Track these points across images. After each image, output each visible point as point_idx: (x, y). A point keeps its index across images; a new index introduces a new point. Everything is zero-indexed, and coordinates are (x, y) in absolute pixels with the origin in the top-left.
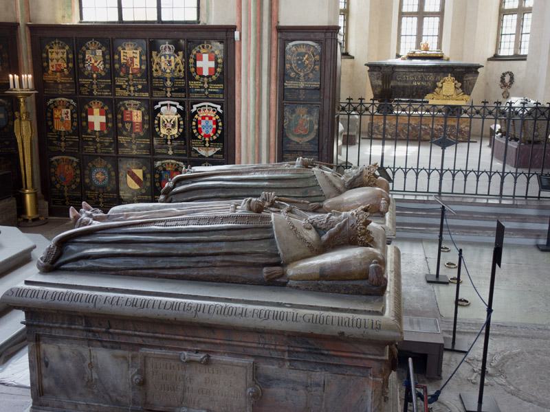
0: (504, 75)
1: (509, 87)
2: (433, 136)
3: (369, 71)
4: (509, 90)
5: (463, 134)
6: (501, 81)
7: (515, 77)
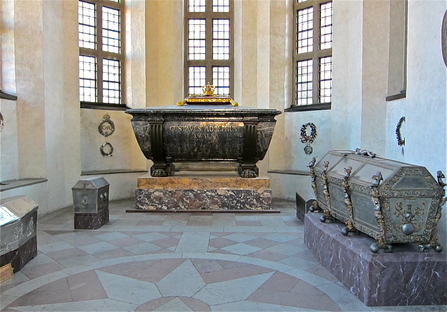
1: (312, 141)
2: (224, 205)
4: (312, 145)
5: (261, 202)
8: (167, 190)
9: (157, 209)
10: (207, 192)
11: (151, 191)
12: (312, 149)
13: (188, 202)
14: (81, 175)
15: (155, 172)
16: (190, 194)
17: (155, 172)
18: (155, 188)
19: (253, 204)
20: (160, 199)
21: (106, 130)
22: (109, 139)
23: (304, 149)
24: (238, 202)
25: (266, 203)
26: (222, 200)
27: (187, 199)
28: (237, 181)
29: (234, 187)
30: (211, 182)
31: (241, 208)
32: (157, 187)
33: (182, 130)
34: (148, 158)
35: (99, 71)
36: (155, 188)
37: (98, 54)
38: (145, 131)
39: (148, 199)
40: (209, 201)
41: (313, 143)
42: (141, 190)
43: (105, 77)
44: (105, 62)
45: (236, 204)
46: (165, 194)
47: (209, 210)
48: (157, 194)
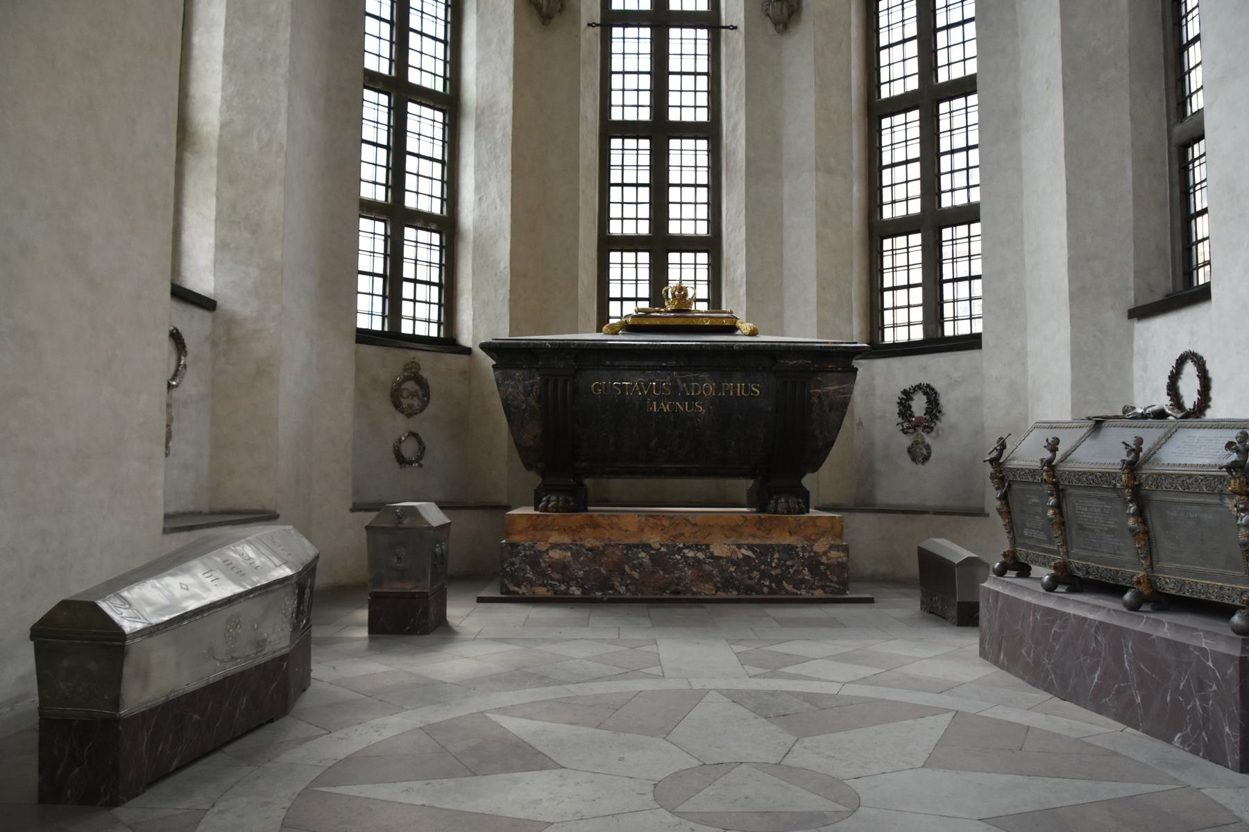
0: (907, 395)
2: (727, 583)
3: (494, 366)
4: (928, 440)
5: (823, 576)
6: (901, 414)
7: (943, 401)
8: (582, 546)
9: (555, 593)
10: (686, 551)
11: (541, 546)
12: (928, 447)
13: (636, 575)
14: (352, 510)
15: (548, 501)
16: (643, 554)
17: (548, 501)
18: (551, 540)
19: (803, 581)
20: (562, 567)
21: (409, 401)
22: (419, 424)
23: (909, 450)
24: (764, 574)
25: (835, 579)
26: (722, 571)
27: (633, 568)
28: (760, 522)
29: (753, 536)
30: (695, 525)
31: (771, 591)
32: (555, 538)
33: (623, 392)
34: (528, 466)
35: (394, 255)
36: (551, 540)
37: (396, 215)
38: (527, 393)
39: (532, 569)
40: (689, 573)
41: (933, 434)
42: (514, 545)
43: (408, 271)
44: (409, 233)
45: (760, 579)
46: (576, 555)
47: (689, 596)
48: (556, 554)
